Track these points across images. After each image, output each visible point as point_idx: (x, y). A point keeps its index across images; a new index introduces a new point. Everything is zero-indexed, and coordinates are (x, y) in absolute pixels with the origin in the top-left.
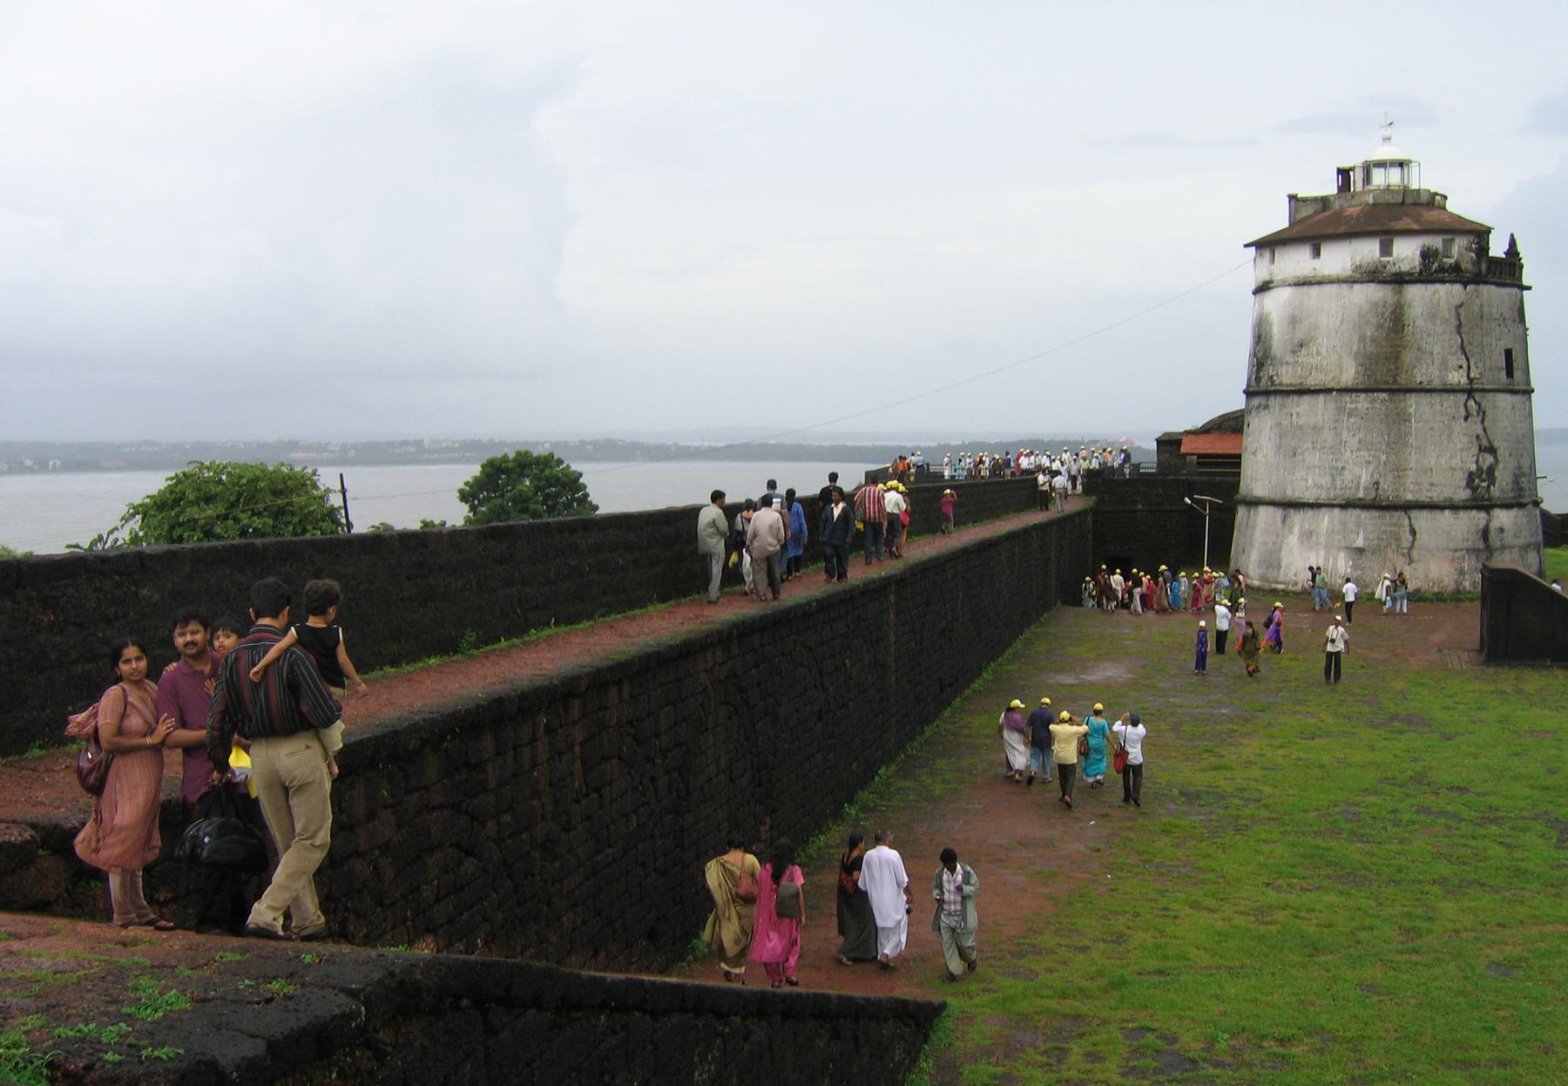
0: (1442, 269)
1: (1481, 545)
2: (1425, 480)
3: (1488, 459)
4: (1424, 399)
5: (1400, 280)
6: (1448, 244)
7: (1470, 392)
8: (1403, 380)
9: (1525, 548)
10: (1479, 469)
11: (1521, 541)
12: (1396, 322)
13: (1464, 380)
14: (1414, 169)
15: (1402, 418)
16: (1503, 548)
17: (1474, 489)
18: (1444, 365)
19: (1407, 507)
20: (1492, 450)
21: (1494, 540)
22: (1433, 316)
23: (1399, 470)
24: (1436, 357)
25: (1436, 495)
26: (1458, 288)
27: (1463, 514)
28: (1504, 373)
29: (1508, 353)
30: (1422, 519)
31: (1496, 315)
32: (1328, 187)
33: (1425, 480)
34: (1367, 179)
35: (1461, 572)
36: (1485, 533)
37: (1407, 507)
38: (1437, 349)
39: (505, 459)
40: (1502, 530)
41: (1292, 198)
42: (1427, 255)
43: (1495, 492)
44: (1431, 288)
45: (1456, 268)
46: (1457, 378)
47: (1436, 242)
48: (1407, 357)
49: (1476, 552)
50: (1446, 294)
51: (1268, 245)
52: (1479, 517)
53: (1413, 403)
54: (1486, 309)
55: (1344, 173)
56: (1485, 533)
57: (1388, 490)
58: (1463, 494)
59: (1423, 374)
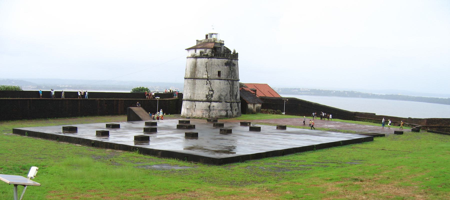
0: (204, 55)
1: (208, 109)
2: (198, 96)
3: (212, 92)
4: (199, 80)
5: (196, 57)
6: (206, 51)
7: (208, 79)
8: (196, 77)
9: (221, 110)
10: (209, 94)
11: (219, 109)
12: (195, 66)
13: (207, 77)
14: (218, 35)
15: (194, 84)
16: (214, 110)
17: (207, 98)
18: (203, 74)
19: (195, 101)
20: (212, 91)
21: (211, 108)
22: (201, 65)
23: (194, 94)
24: (202, 73)
25: (200, 99)
26: (207, 59)
27: (204, 103)
28: (217, 77)
29: (219, 73)
30: (197, 103)
31: (216, 64)
32: (203, 38)
33: (198, 96)
34: (211, 37)
35: (203, 114)
36: (209, 107)
37: (195, 101)
38: (202, 71)
39: (138, 88)
40: (214, 106)
41: (197, 41)
42: (201, 53)
43: (213, 99)
44: (201, 59)
45: (207, 55)
46: (205, 76)
47: (203, 50)
48: (197, 72)
49: (207, 110)
50: (205, 60)
51: (188, 49)
52: (209, 104)
53: (197, 81)
54: (213, 63)
55: (207, 36)
56: (209, 107)
57: (192, 98)
58: (205, 99)
59: (199, 75)
